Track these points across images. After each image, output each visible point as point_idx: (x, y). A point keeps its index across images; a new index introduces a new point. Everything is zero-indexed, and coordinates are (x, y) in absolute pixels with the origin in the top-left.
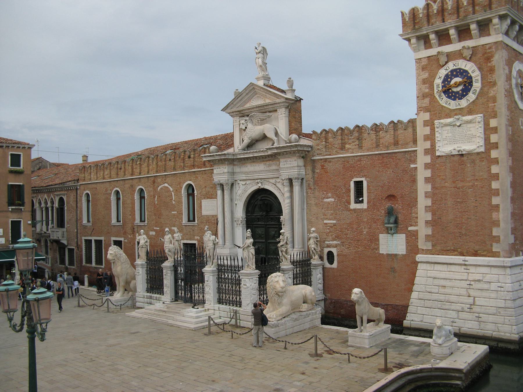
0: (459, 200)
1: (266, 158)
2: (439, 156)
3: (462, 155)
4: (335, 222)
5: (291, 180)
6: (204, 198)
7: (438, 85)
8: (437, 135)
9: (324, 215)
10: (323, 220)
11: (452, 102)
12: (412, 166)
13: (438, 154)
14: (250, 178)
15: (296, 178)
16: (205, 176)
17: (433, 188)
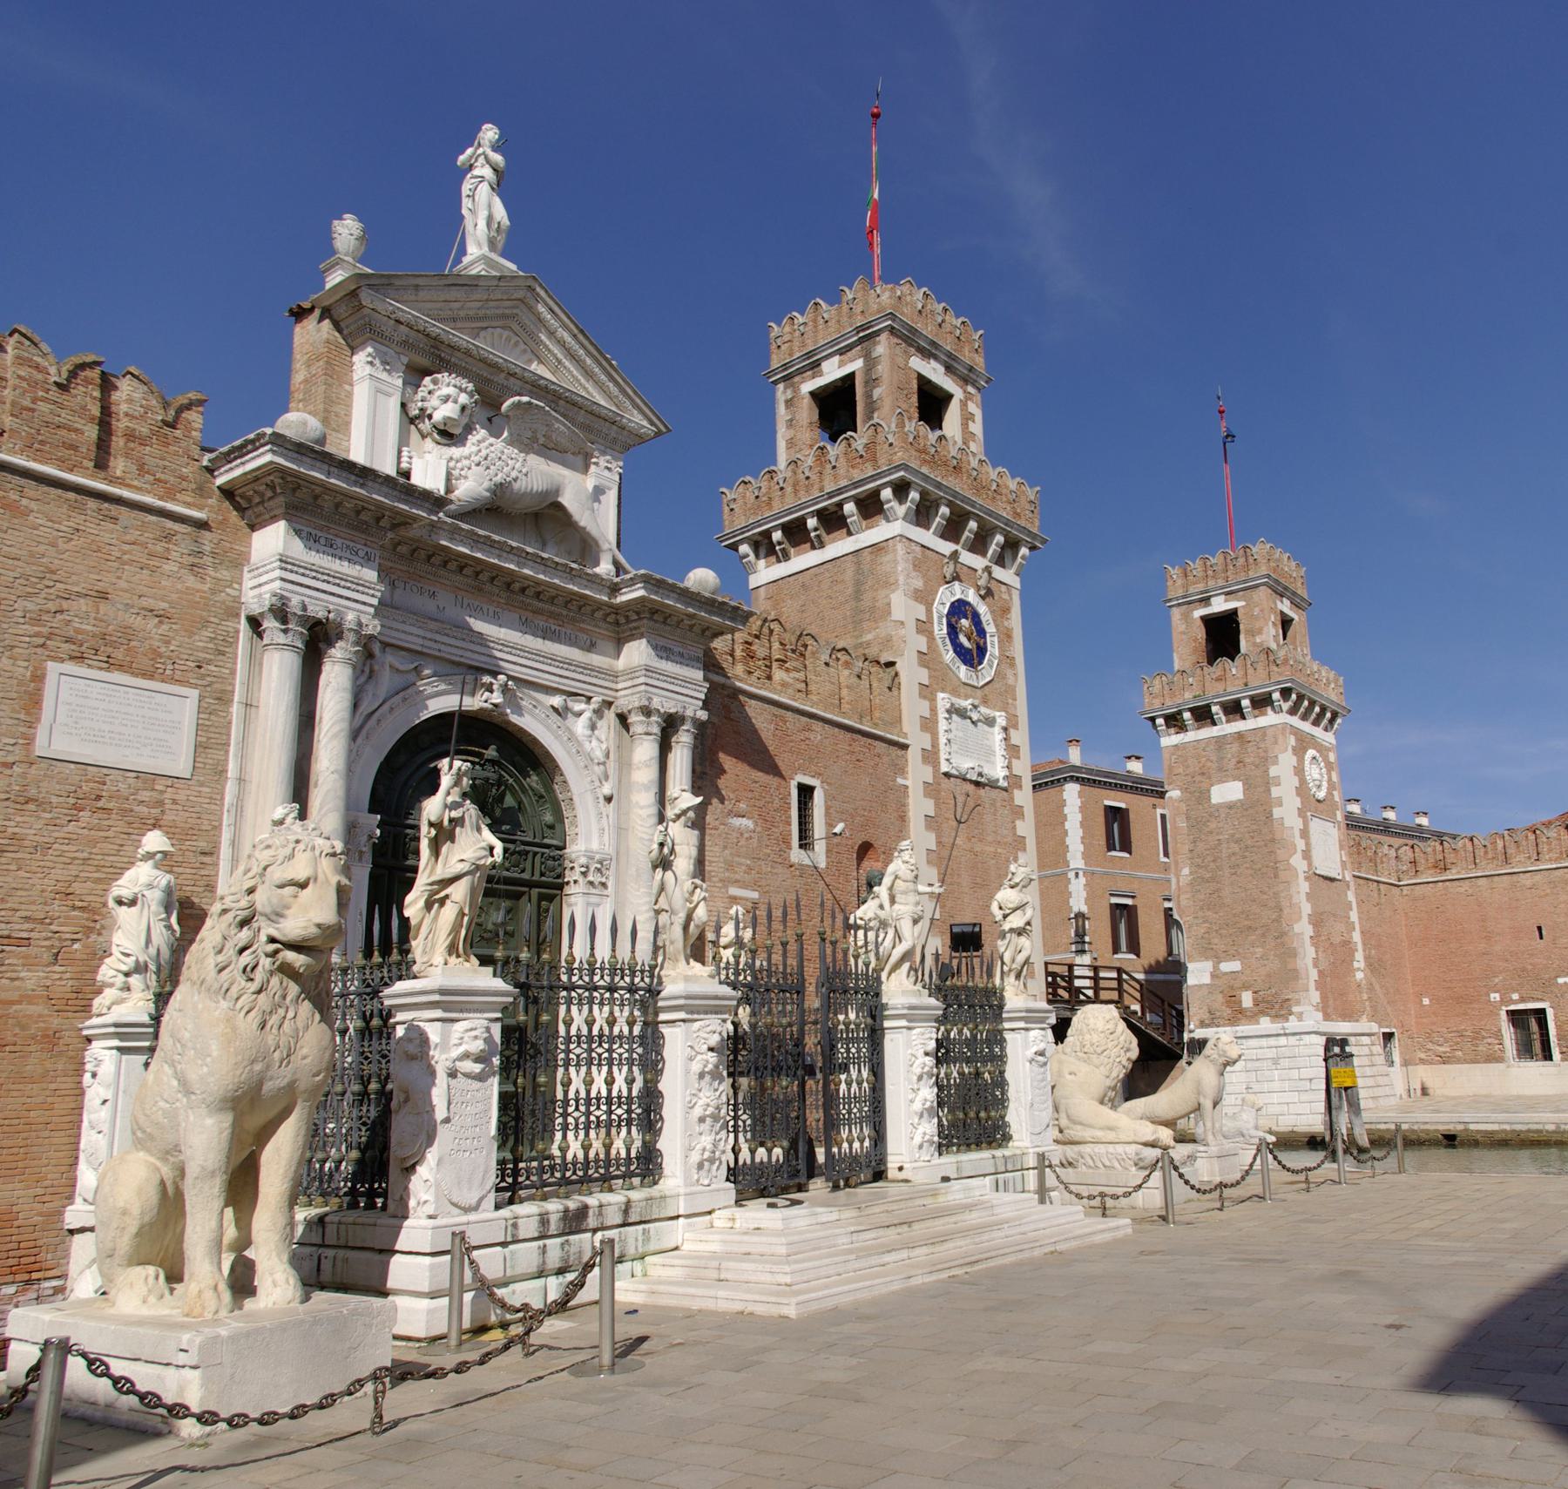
0: (979, 880)
1: (552, 600)
2: (947, 775)
3: (977, 784)
4: (755, 895)
5: (670, 724)
6: (79, 658)
7: (940, 618)
8: (943, 725)
9: (730, 866)
10: (726, 883)
11: (963, 668)
12: (900, 781)
13: (944, 768)
14: (447, 652)
15: (695, 721)
16: (107, 533)
17: (939, 843)
